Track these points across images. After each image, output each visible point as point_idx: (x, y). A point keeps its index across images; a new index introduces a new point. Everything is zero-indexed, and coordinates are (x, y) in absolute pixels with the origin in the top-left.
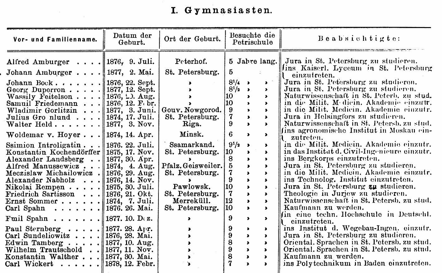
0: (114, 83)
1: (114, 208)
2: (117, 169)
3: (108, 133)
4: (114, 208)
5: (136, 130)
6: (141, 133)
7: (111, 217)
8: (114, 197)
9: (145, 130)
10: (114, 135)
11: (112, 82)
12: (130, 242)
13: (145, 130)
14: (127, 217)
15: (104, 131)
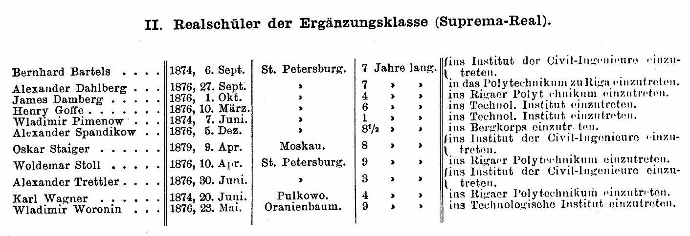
0: (182, 87)
1: (182, 208)
2: (187, 125)
3: (172, 68)
4: (182, 208)
5: (216, 141)
6: (222, 144)
7: (178, 195)
8: (181, 114)
9: (229, 140)
10: (182, 70)
11: (178, 86)
12: (208, 107)
13: (229, 140)
14: (202, 161)
15: (165, 81)
